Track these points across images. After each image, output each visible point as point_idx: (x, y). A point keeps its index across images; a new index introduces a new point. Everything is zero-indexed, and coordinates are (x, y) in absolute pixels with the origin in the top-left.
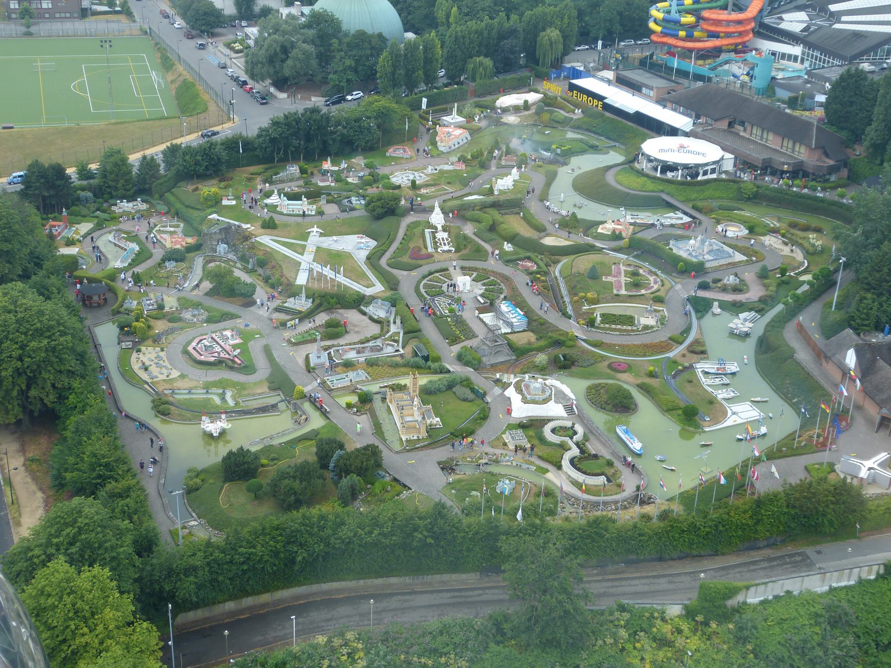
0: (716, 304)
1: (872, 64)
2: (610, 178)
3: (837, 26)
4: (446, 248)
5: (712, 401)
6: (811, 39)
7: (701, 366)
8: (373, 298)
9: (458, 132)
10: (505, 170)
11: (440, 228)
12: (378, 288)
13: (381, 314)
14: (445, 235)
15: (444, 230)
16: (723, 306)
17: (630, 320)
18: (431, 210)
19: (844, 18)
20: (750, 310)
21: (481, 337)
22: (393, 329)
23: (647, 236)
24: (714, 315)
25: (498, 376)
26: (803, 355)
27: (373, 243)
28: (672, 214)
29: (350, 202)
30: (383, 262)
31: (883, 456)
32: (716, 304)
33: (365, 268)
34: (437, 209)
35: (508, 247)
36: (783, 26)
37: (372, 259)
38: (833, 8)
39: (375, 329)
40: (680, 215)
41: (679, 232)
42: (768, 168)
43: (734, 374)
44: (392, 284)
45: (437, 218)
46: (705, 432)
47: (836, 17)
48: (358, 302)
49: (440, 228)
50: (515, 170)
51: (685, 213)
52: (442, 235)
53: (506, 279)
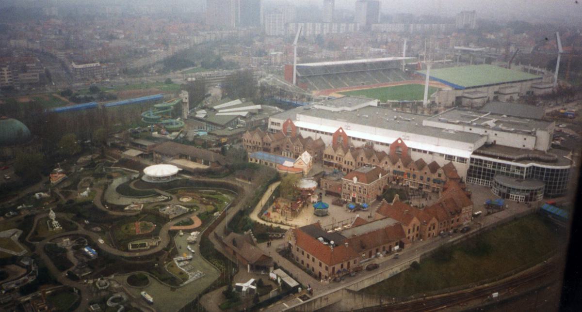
0: (181, 231)
1: (231, 127)
2: (132, 186)
3: (217, 114)
4: (58, 227)
5: (181, 273)
6: (208, 119)
7: (176, 259)
8: (22, 257)
9: (61, 175)
10: (84, 188)
11: (53, 219)
12: (24, 251)
13: (27, 263)
14: (57, 222)
15: (56, 220)
16: (184, 231)
17: (144, 245)
18: (49, 211)
19: (220, 111)
20: (195, 231)
21: (76, 265)
22: (33, 268)
23: (150, 207)
24: (181, 236)
25: (85, 281)
26: (218, 246)
27: (20, 232)
28: (160, 197)
29: (9, 214)
30: (27, 239)
31: (252, 280)
32: (181, 231)
33: (18, 243)
34: (52, 211)
35: (87, 222)
36: (197, 116)
37: (21, 239)
38: (215, 107)
39: (24, 271)
40: (163, 197)
41: (163, 203)
42: (199, 172)
43: (191, 260)
44: (32, 248)
45: (52, 215)
46: (181, 287)
47: (216, 111)
48: (14, 260)
49: (53, 219)
50: (88, 189)
51: (164, 195)
52: (55, 222)
53: (87, 237)
